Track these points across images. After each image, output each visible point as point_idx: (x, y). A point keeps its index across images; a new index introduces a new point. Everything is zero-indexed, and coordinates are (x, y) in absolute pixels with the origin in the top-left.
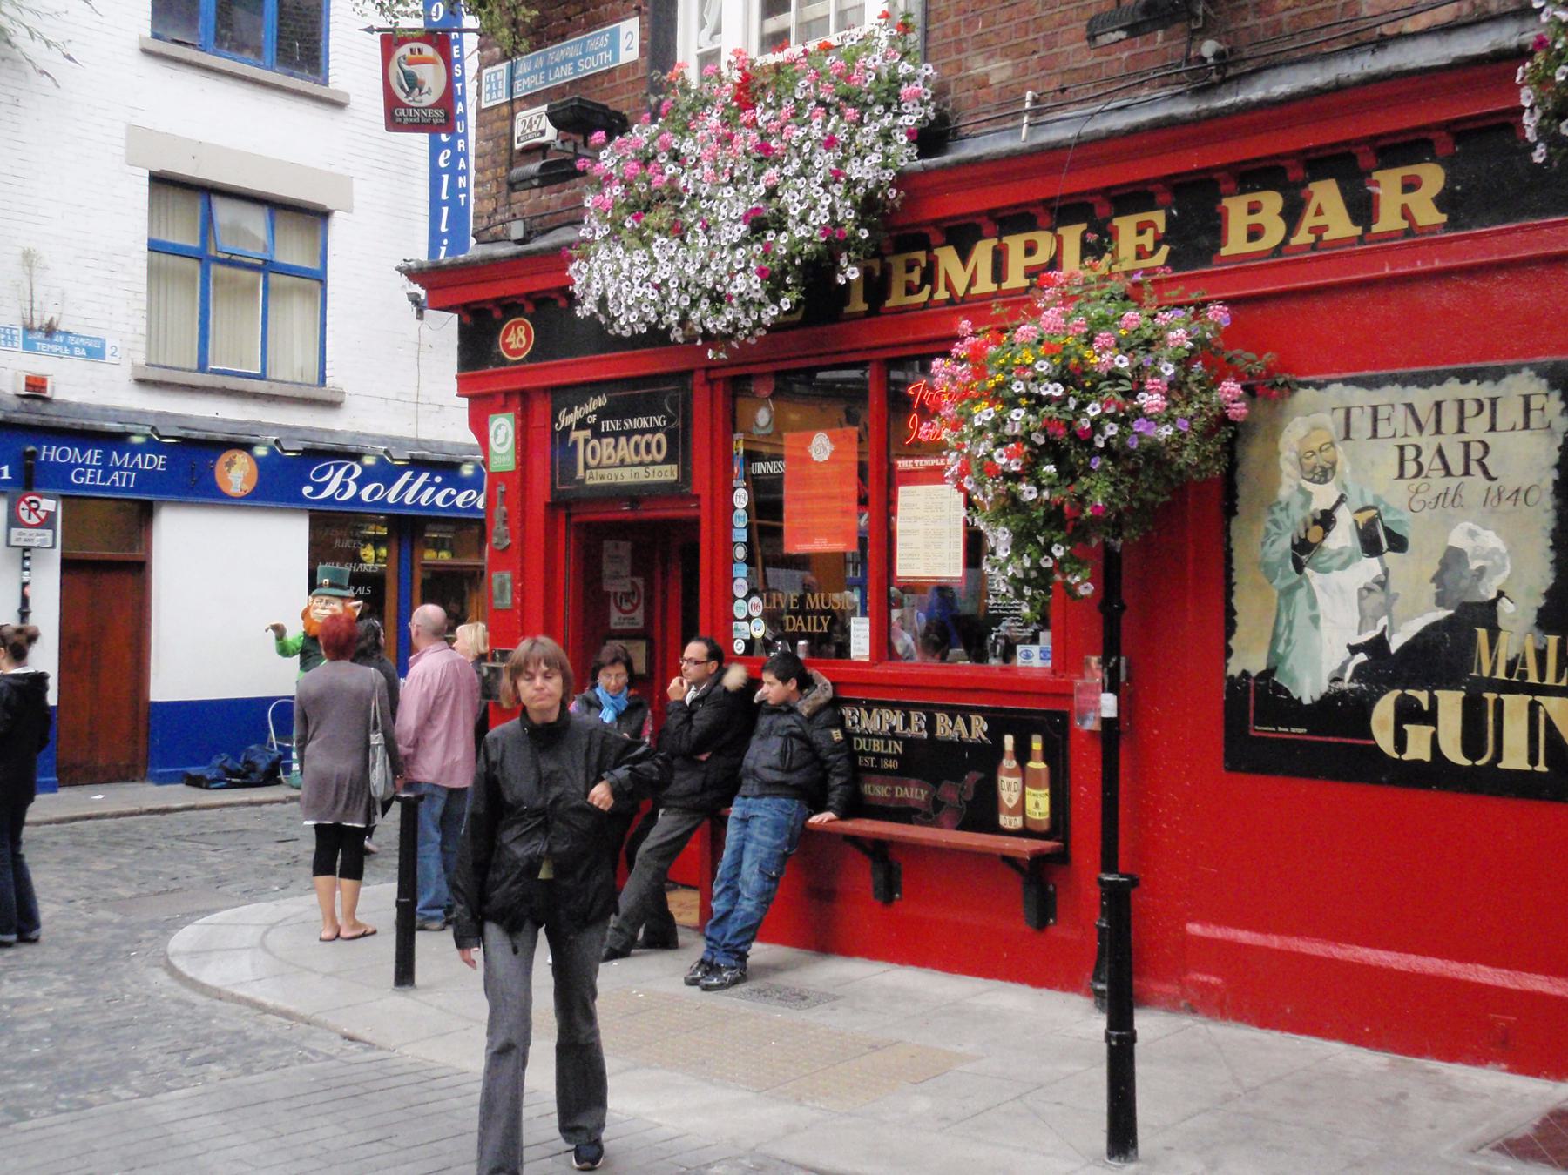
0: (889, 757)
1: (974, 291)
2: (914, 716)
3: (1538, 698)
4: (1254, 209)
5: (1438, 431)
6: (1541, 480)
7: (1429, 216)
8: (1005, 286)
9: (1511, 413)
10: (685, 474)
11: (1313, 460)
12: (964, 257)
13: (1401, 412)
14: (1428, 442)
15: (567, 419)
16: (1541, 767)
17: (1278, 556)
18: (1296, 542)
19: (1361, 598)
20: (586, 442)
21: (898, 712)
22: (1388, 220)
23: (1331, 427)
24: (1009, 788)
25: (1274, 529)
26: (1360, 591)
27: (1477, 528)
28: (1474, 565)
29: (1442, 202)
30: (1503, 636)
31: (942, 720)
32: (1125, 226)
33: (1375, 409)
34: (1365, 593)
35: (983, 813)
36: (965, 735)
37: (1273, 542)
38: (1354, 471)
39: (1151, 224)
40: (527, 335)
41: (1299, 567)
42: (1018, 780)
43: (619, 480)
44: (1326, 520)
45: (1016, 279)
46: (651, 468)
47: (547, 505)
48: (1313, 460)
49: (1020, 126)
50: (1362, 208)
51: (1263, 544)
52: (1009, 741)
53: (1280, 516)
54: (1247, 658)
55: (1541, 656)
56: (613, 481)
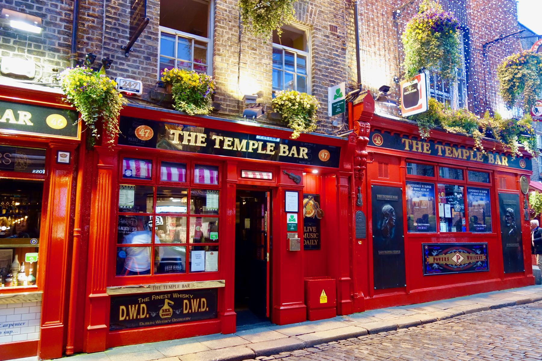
4: (491, 157)
7: (507, 165)
12: (457, 151)
45: (465, 158)
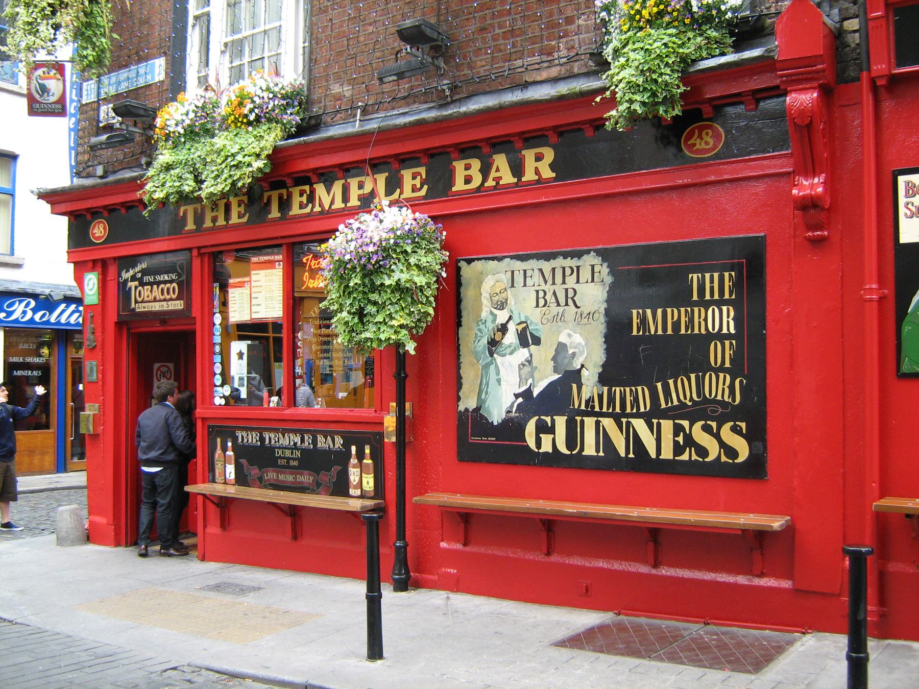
0: (294, 459)
1: (333, 207)
2: (306, 437)
3: (599, 419)
4: (467, 167)
5: (554, 283)
6: (600, 308)
7: (548, 174)
8: (348, 205)
9: (585, 274)
10: (188, 305)
11: (497, 298)
13: (537, 272)
14: (549, 288)
15: (126, 275)
16: (601, 454)
17: (481, 347)
18: (490, 341)
19: (520, 369)
20: (136, 288)
21: (298, 435)
22: (529, 175)
23: (505, 281)
24: (354, 475)
25: (479, 334)
26: (519, 365)
27: (571, 333)
28: (571, 351)
29: (553, 167)
30: (584, 387)
31: (320, 438)
32: (407, 174)
33: (525, 271)
34: (521, 366)
35: (341, 488)
36: (332, 446)
37: (479, 341)
38: (515, 303)
39: (419, 174)
40: (105, 228)
41: (491, 354)
42: (359, 470)
43: (153, 309)
44: (503, 329)
45: (354, 202)
46: (170, 303)
47: (116, 323)
48: (497, 298)
49: (355, 121)
50: (517, 169)
51: (474, 342)
52: (354, 448)
53: (482, 327)
54: (468, 402)
55: (600, 397)
56: (150, 309)
